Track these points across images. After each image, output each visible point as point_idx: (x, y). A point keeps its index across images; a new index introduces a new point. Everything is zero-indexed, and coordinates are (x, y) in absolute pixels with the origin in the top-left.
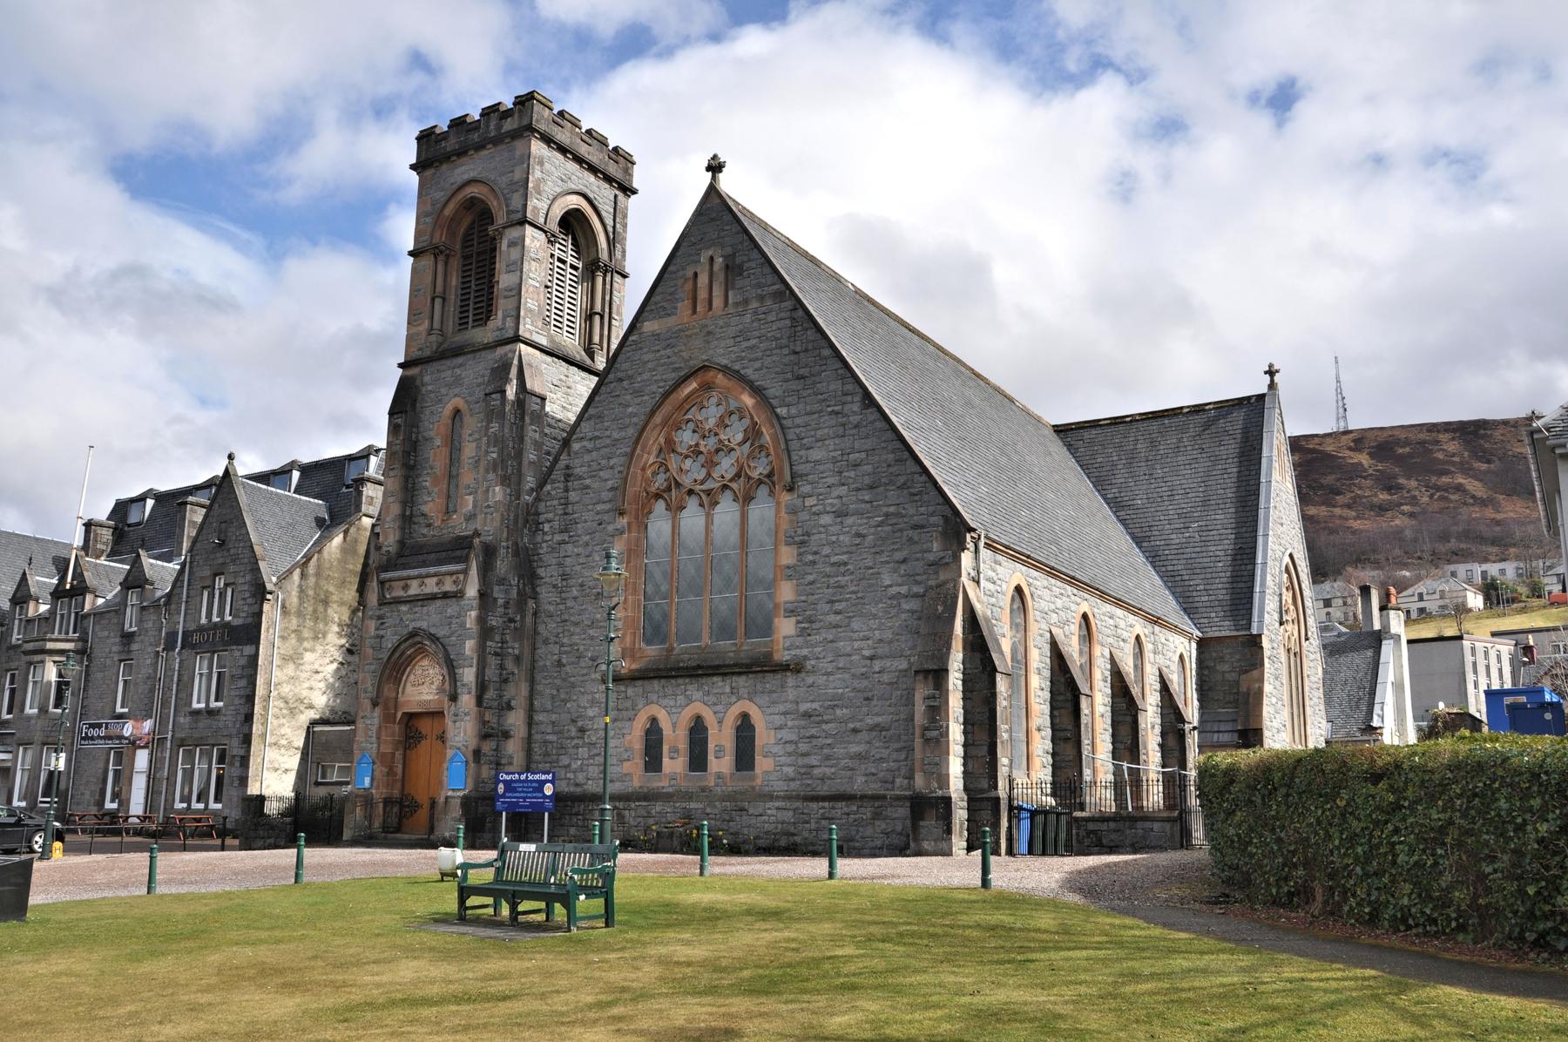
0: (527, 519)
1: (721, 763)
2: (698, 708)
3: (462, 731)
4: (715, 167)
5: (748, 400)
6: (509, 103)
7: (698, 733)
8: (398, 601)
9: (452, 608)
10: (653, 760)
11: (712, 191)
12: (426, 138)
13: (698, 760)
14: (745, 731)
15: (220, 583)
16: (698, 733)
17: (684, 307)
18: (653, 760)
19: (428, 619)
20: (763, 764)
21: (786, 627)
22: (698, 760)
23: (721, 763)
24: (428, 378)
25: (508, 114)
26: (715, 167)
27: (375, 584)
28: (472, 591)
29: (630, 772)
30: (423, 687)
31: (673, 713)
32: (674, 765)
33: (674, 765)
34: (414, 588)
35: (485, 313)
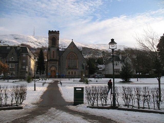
0: (60, 59)
1: (74, 74)
2: (72, 71)
3: (57, 71)
4: (72, 40)
5: (75, 54)
6: (57, 31)
7: (72, 72)
8: (51, 63)
9: (56, 64)
10: (69, 73)
11: (72, 41)
12: (49, 31)
13: (72, 73)
14: (75, 72)
15: (12, 57)
16: (72, 72)
17: (71, 48)
18: (69, 73)
19: (54, 65)
20: (76, 74)
21: (77, 67)
22: (72, 73)
23: (74, 74)
24: (51, 48)
25: (57, 32)
26: (72, 40)
27: (49, 62)
28: (58, 63)
29: (68, 74)
30: (53, 69)
31: (70, 71)
32: (71, 74)
33: (71, 74)
34: (53, 62)
35: (55, 45)
